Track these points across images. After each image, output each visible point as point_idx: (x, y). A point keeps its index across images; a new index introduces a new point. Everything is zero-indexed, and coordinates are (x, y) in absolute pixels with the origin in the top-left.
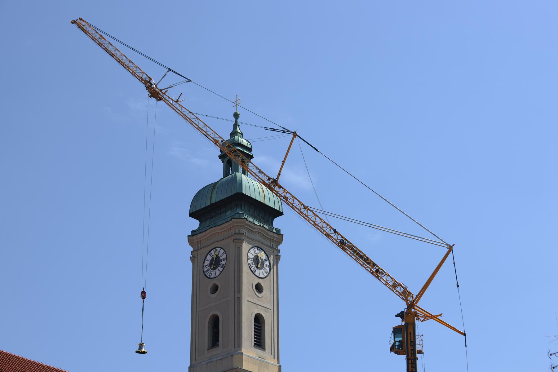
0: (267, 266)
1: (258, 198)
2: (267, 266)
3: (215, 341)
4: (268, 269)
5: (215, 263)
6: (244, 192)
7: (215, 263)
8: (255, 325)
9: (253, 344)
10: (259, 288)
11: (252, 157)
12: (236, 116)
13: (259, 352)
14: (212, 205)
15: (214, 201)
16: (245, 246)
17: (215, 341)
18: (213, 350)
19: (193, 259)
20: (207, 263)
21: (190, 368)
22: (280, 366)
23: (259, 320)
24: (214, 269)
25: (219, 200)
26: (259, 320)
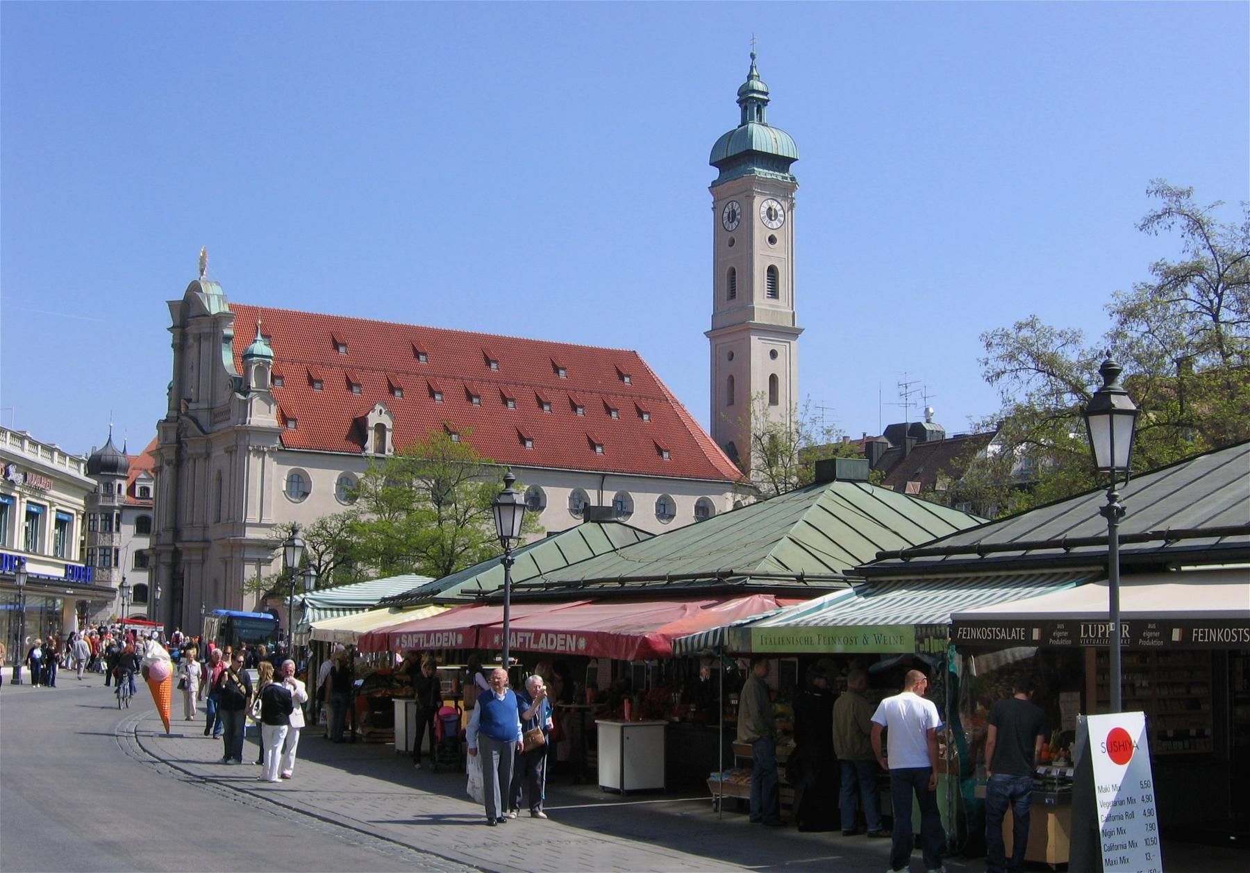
0: (781, 216)
1: (770, 151)
2: (781, 216)
3: (732, 295)
4: (782, 219)
5: (733, 216)
6: (754, 148)
7: (733, 216)
8: (768, 276)
9: (766, 295)
10: (772, 240)
11: (768, 101)
12: (753, 56)
13: (773, 301)
14: (727, 158)
15: (729, 155)
16: (757, 200)
17: (732, 295)
18: (731, 301)
19: (714, 209)
20: (725, 215)
21: (712, 316)
22: (794, 313)
23: (772, 272)
24: (733, 221)
25: (733, 154)
26: (772, 272)
